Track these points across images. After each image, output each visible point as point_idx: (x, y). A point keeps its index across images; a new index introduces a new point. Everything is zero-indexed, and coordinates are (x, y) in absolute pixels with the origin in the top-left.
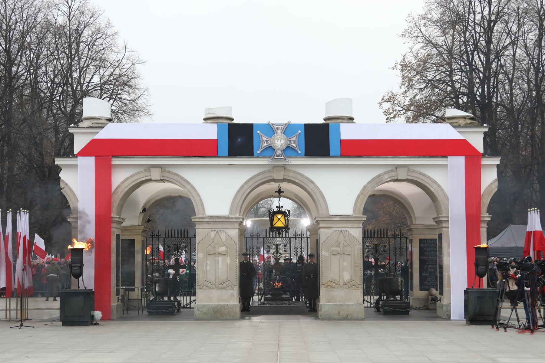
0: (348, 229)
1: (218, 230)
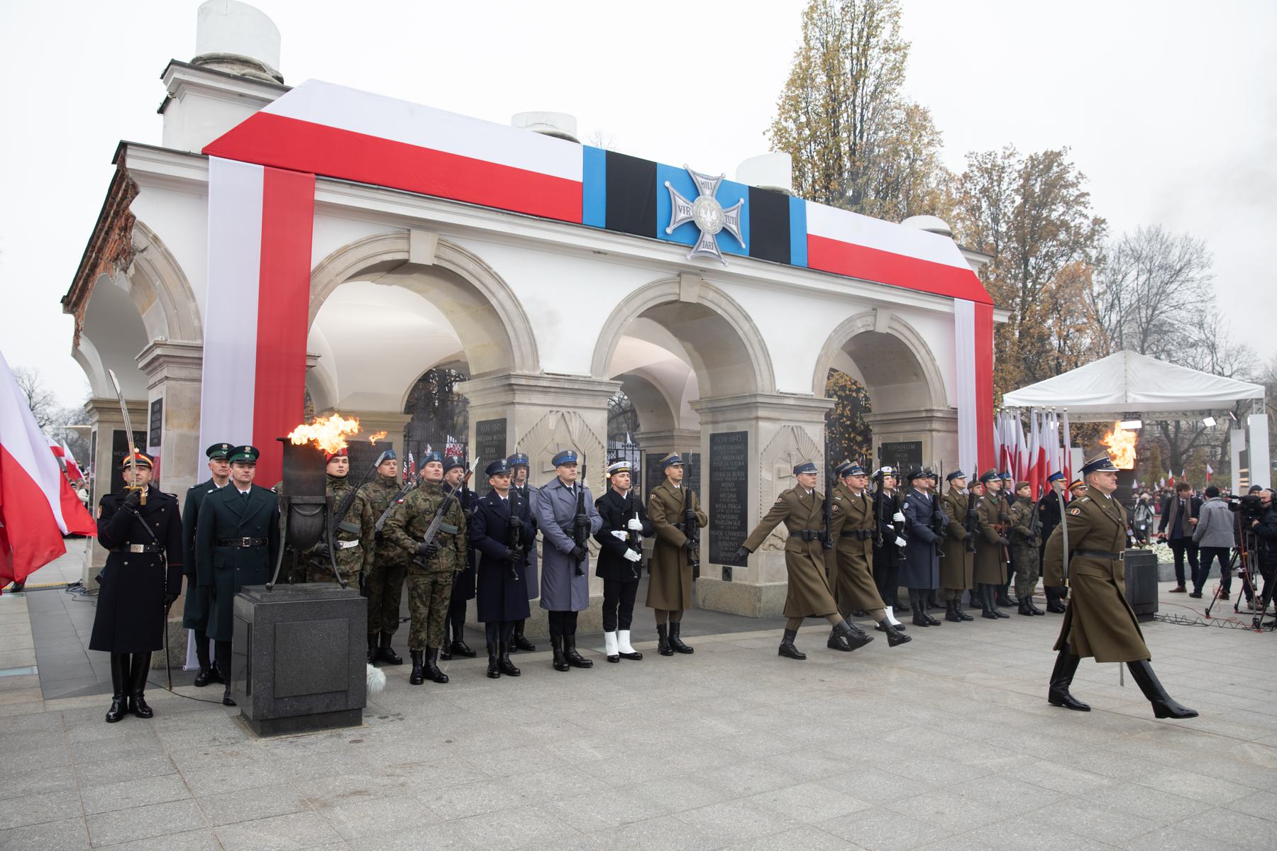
0: (802, 425)
1: (564, 410)
